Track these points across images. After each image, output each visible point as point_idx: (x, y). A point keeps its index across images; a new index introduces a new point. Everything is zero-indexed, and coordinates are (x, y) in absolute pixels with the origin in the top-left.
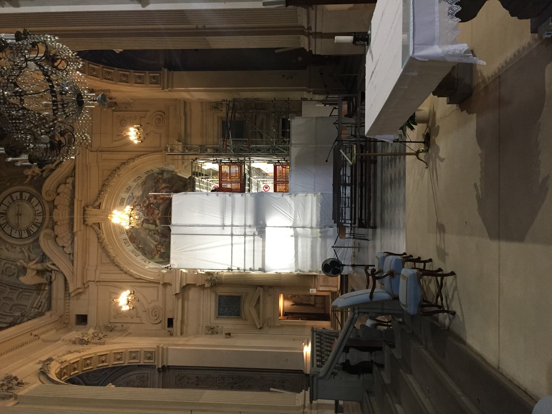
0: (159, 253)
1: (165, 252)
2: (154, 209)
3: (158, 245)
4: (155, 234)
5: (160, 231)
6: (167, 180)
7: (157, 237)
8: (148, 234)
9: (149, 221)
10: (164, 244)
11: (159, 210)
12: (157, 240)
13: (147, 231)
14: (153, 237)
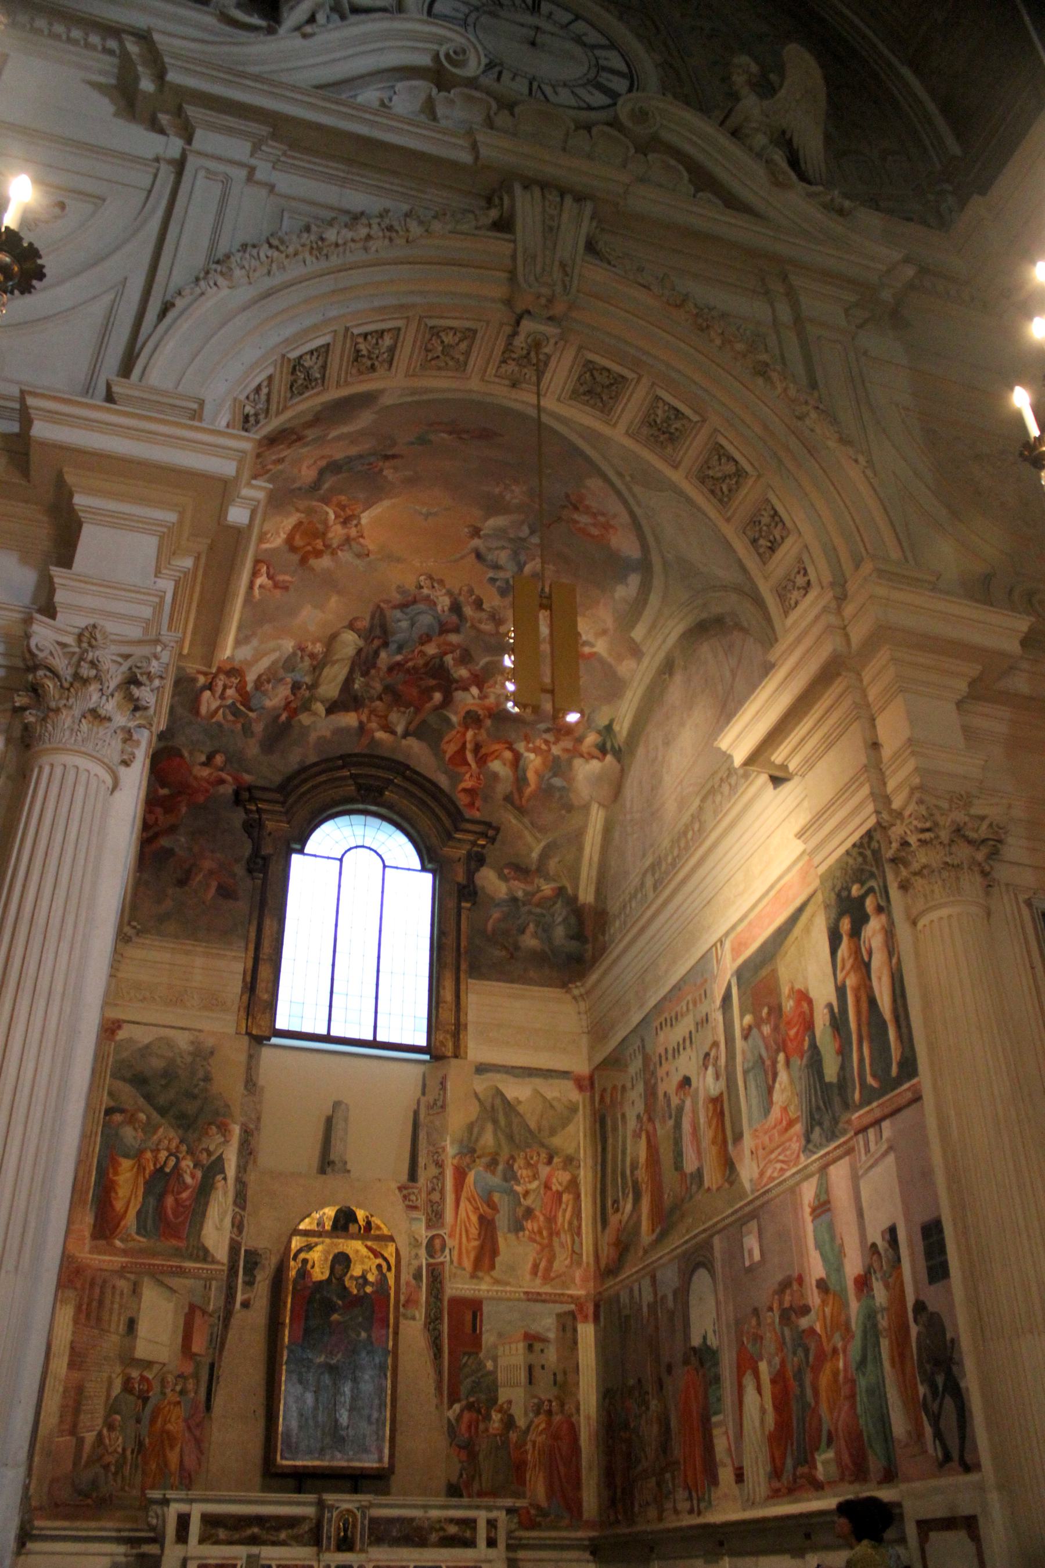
0: (202, 680)
1: (196, 712)
2: (418, 710)
3: (241, 689)
4: (296, 687)
5: (305, 719)
6: (557, 782)
7: (277, 697)
8: (302, 650)
9: (365, 674)
10: (239, 726)
11: (406, 734)
12: (265, 693)
13: (319, 648)
14: (281, 673)
